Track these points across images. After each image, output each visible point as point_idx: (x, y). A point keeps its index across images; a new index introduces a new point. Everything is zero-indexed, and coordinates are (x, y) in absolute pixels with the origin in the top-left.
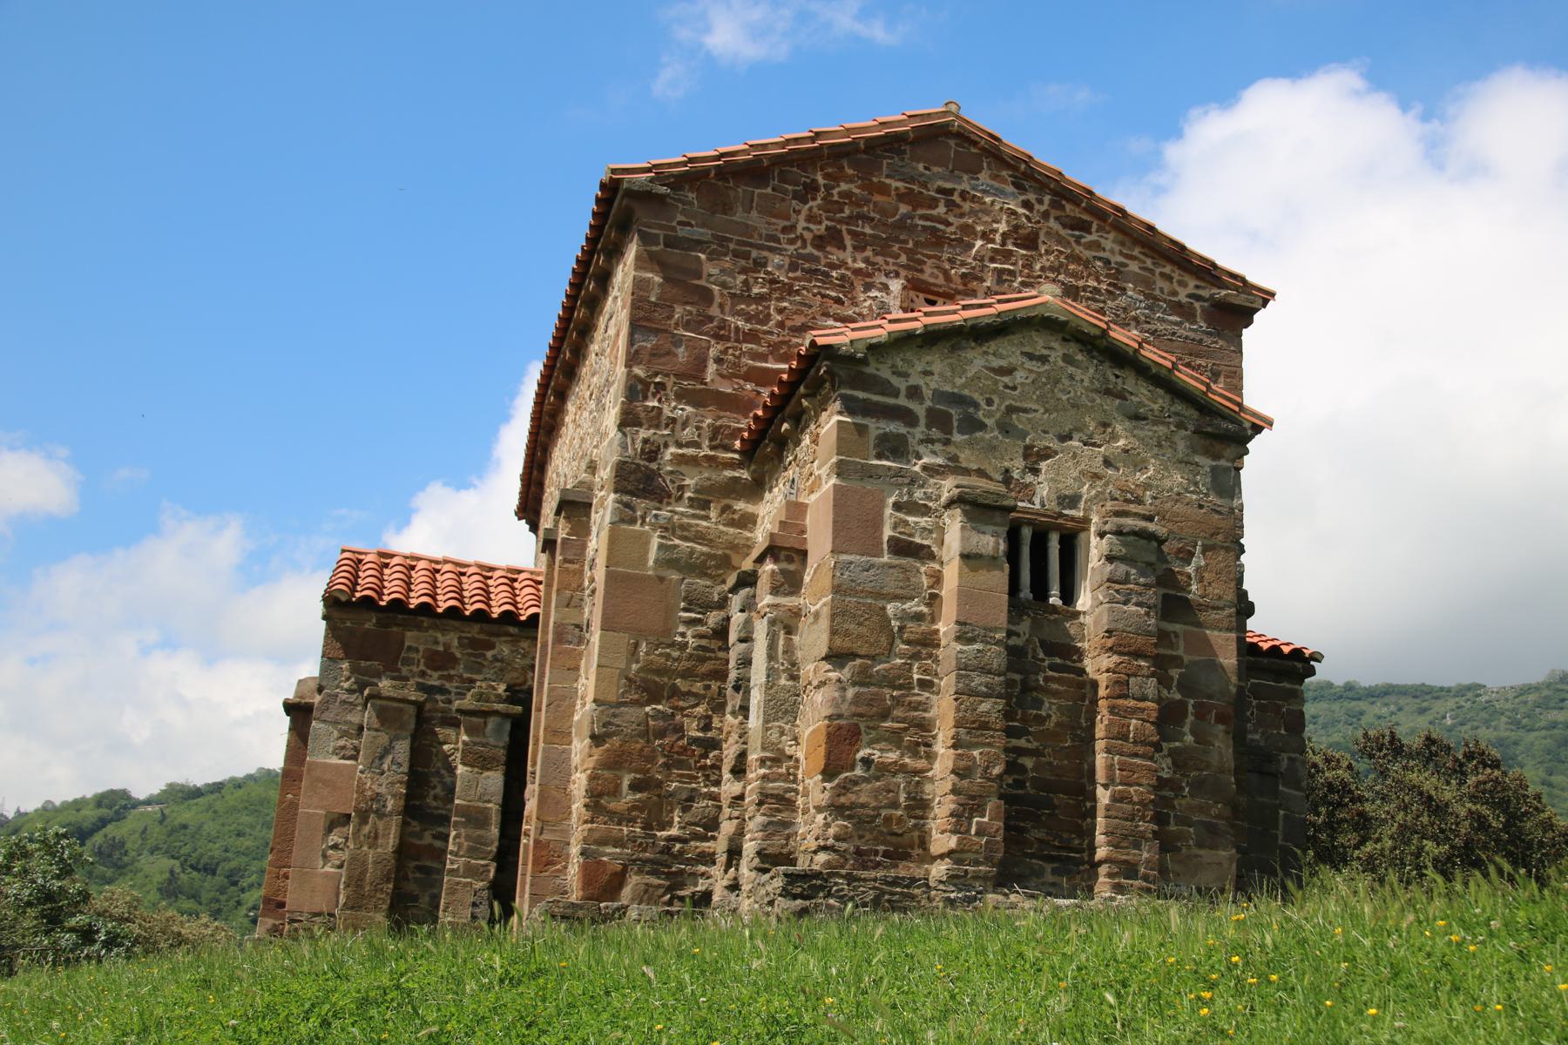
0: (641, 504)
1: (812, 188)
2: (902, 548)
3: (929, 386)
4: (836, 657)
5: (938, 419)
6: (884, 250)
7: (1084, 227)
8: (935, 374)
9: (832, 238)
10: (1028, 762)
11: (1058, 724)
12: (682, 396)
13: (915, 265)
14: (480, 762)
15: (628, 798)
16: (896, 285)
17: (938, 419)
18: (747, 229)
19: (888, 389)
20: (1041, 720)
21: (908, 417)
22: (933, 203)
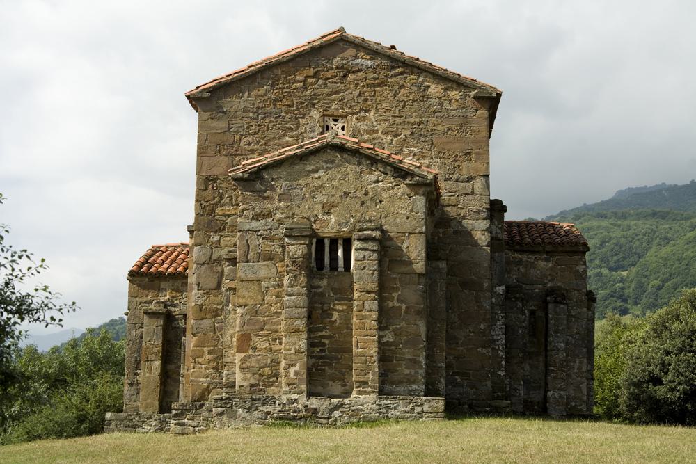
10: (327, 342)
11: (340, 323)
15: (207, 356)
20: (333, 322)
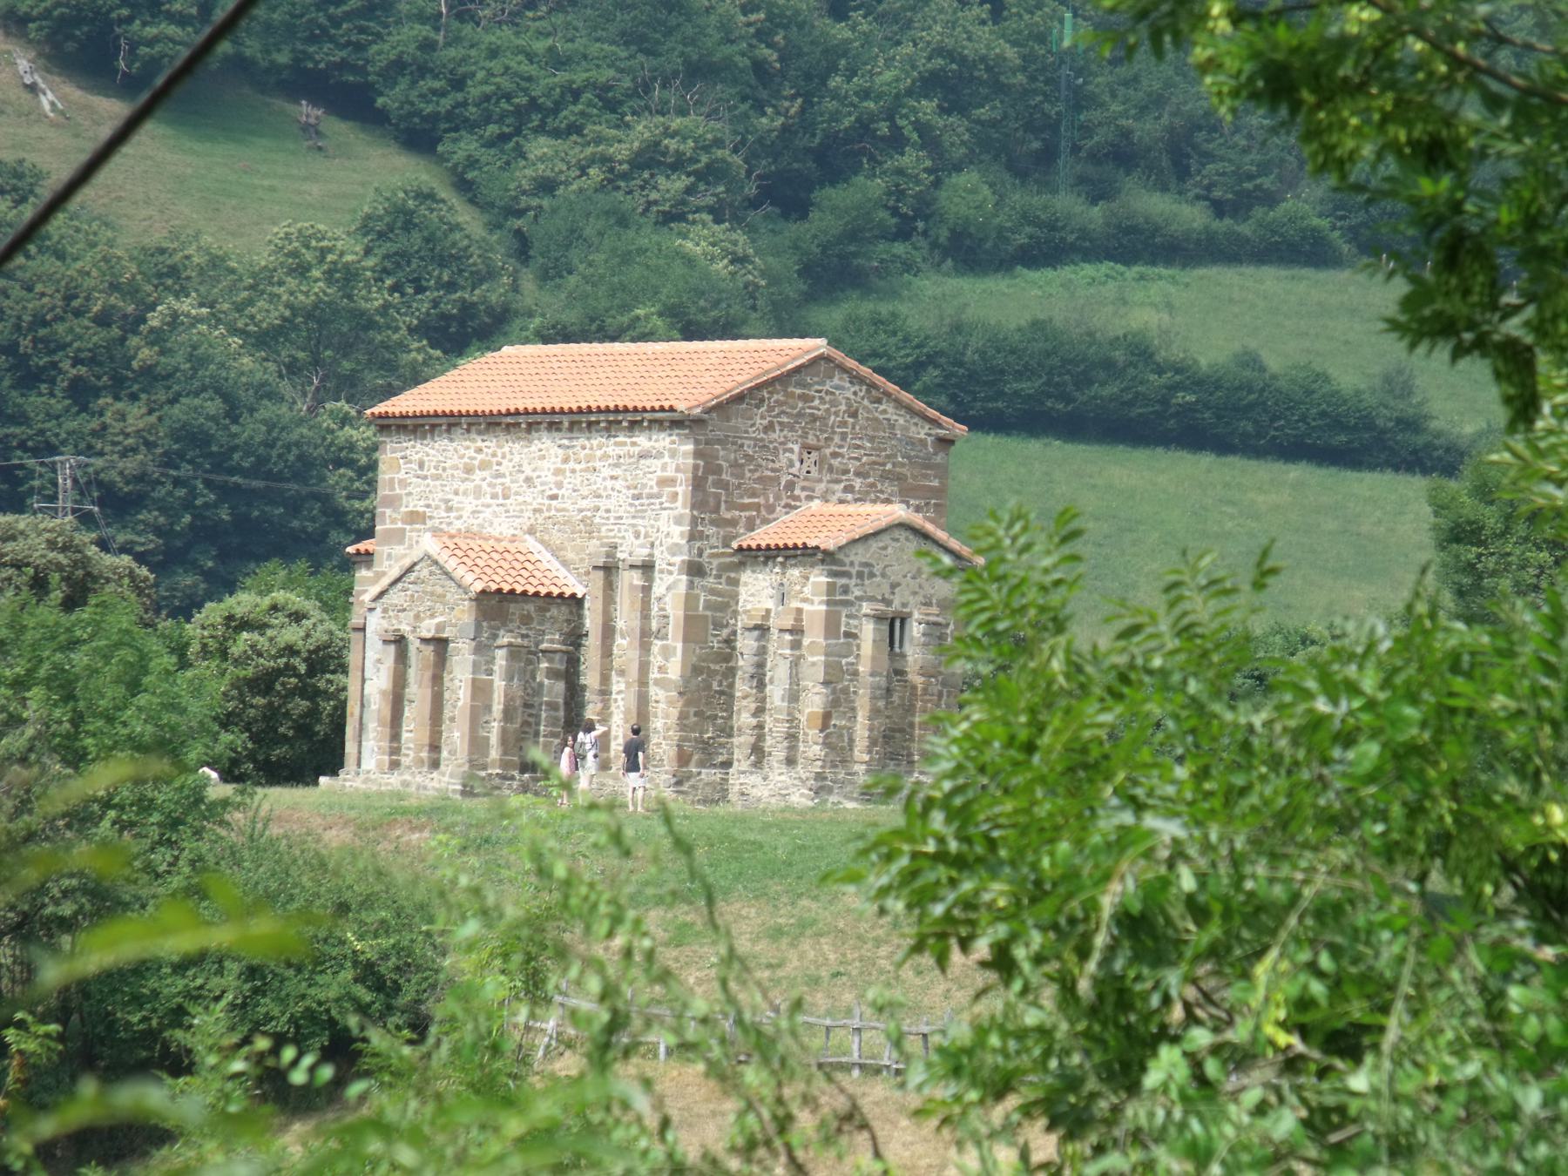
0: (697, 580)
1: (762, 400)
2: (848, 635)
3: (858, 559)
4: (826, 683)
5: (860, 575)
6: (792, 429)
7: (879, 401)
8: (858, 556)
9: (769, 428)
12: (713, 523)
13: (805, 435)
14: (552, 674)
16: (796, 448)
17: (860, 575)
18: (736, 429)
19: (842, 564)
21: (847, 574)
22: (812, 399)
